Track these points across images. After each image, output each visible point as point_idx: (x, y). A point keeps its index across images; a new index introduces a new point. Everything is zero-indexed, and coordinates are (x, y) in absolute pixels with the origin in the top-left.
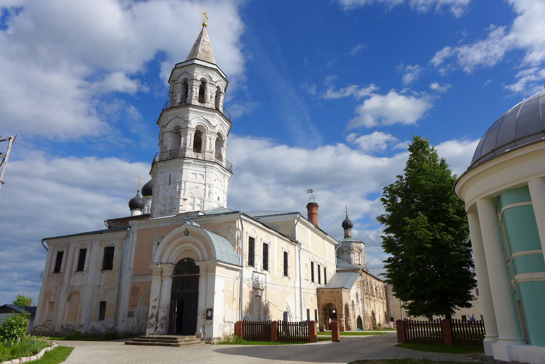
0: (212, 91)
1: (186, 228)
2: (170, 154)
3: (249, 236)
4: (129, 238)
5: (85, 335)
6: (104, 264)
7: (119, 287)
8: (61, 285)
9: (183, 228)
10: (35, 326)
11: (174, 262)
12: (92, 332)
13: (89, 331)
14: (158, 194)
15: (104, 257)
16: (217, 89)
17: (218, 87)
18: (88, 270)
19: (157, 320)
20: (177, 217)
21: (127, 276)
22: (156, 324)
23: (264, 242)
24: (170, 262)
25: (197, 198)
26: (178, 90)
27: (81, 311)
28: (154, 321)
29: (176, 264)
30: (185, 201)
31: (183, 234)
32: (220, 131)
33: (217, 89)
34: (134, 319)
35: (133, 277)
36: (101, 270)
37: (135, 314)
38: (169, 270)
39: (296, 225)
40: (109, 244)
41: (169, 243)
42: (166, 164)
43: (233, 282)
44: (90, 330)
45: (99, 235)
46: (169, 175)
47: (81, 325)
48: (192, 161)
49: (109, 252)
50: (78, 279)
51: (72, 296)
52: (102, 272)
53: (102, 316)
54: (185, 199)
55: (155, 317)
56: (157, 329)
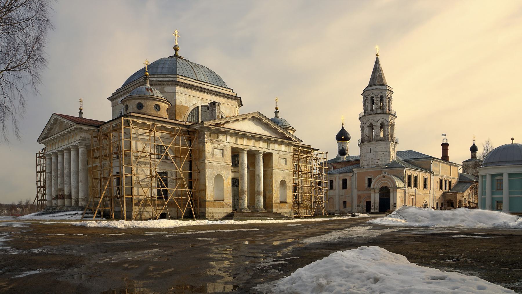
1: (384, 175)
7: (352, 196)
9: (382, 175)
14: (365, 157)
24: (377, 187)
26: (369, 103)
27: (335, 205)
34: (361, 207)
37: (360, 205)
38: (377, 191)
39: (431, 164)
40: (344, 178)
48: (380, 142)
49: (345, 182)
53: (345, 207)
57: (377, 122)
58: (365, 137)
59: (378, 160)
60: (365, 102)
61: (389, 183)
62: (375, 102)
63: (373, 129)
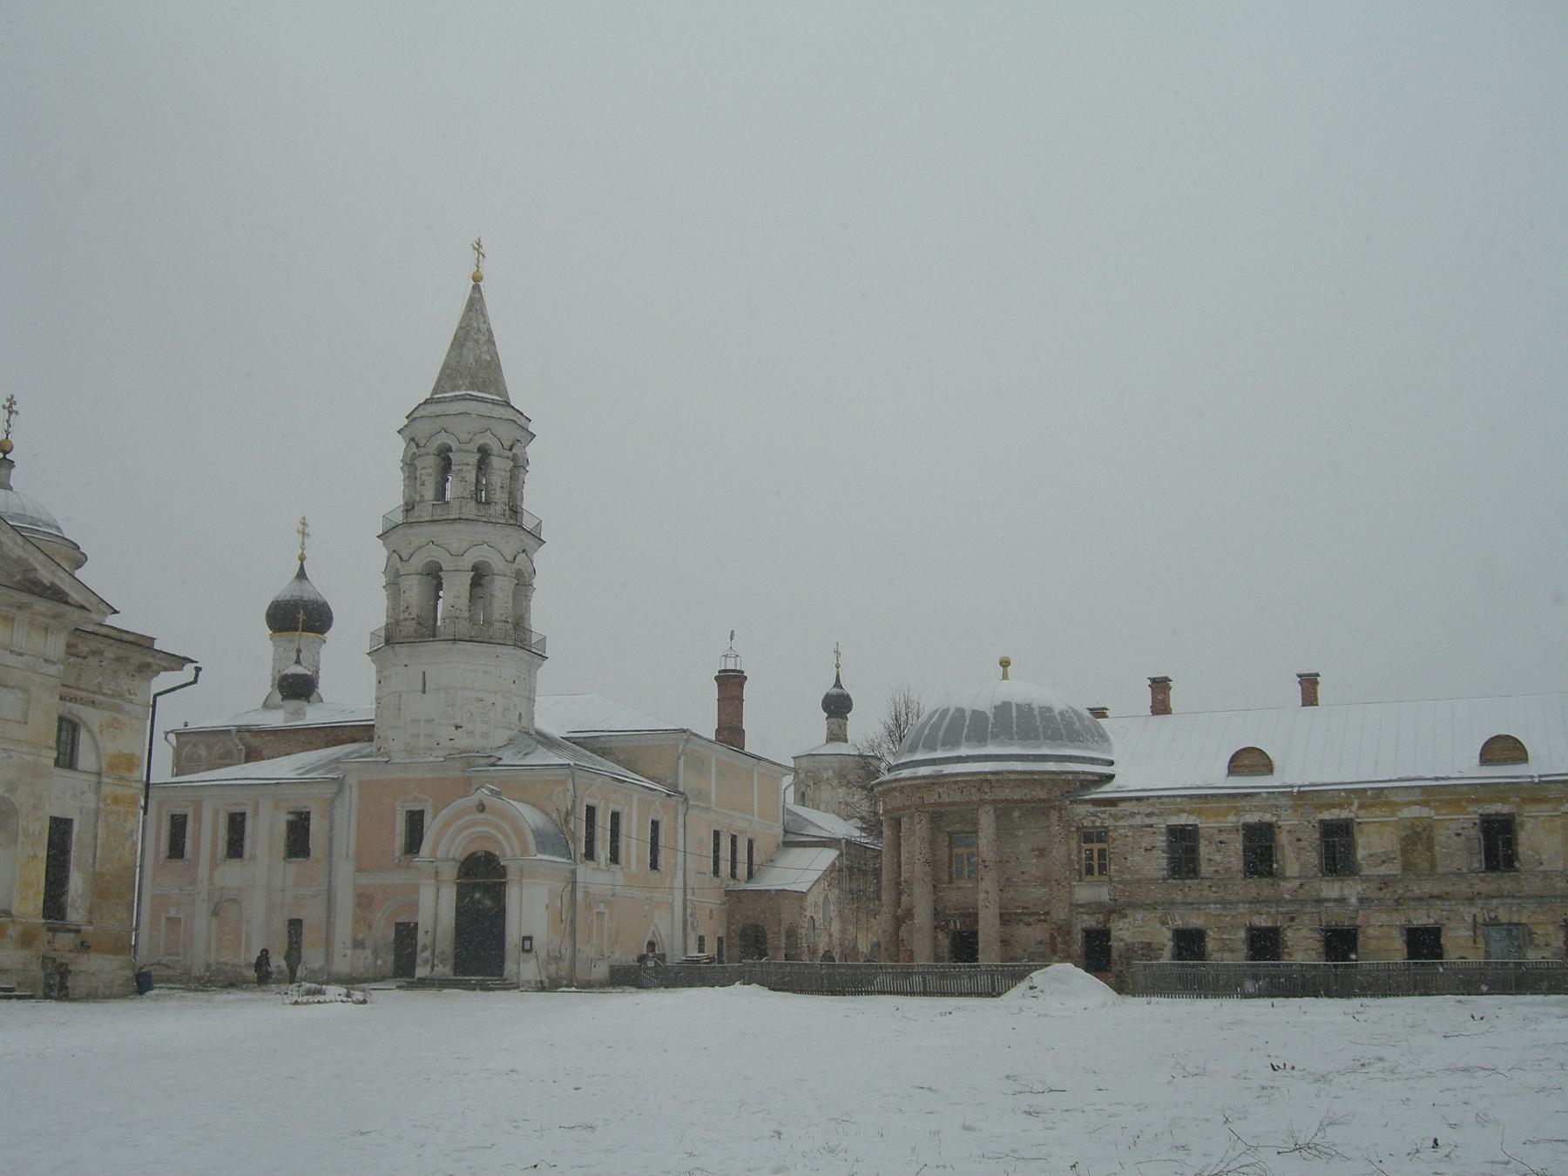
9: (474, 799)
10: (142, 965)
11: (457, 858)
14: (399, 709)
18: (253, 858)
21: (345, 872)
24: (451, 856)
29: (462, 859)
30: (459, 729)
31: (475, 809)
38: (450, 872)
41: (447, 825)
50: (232, 874)
56: (436, 968)
58: (402, 618)
59: (457, 727)
60: (410, 464)
61: (500, 836)
63: (439, 586)
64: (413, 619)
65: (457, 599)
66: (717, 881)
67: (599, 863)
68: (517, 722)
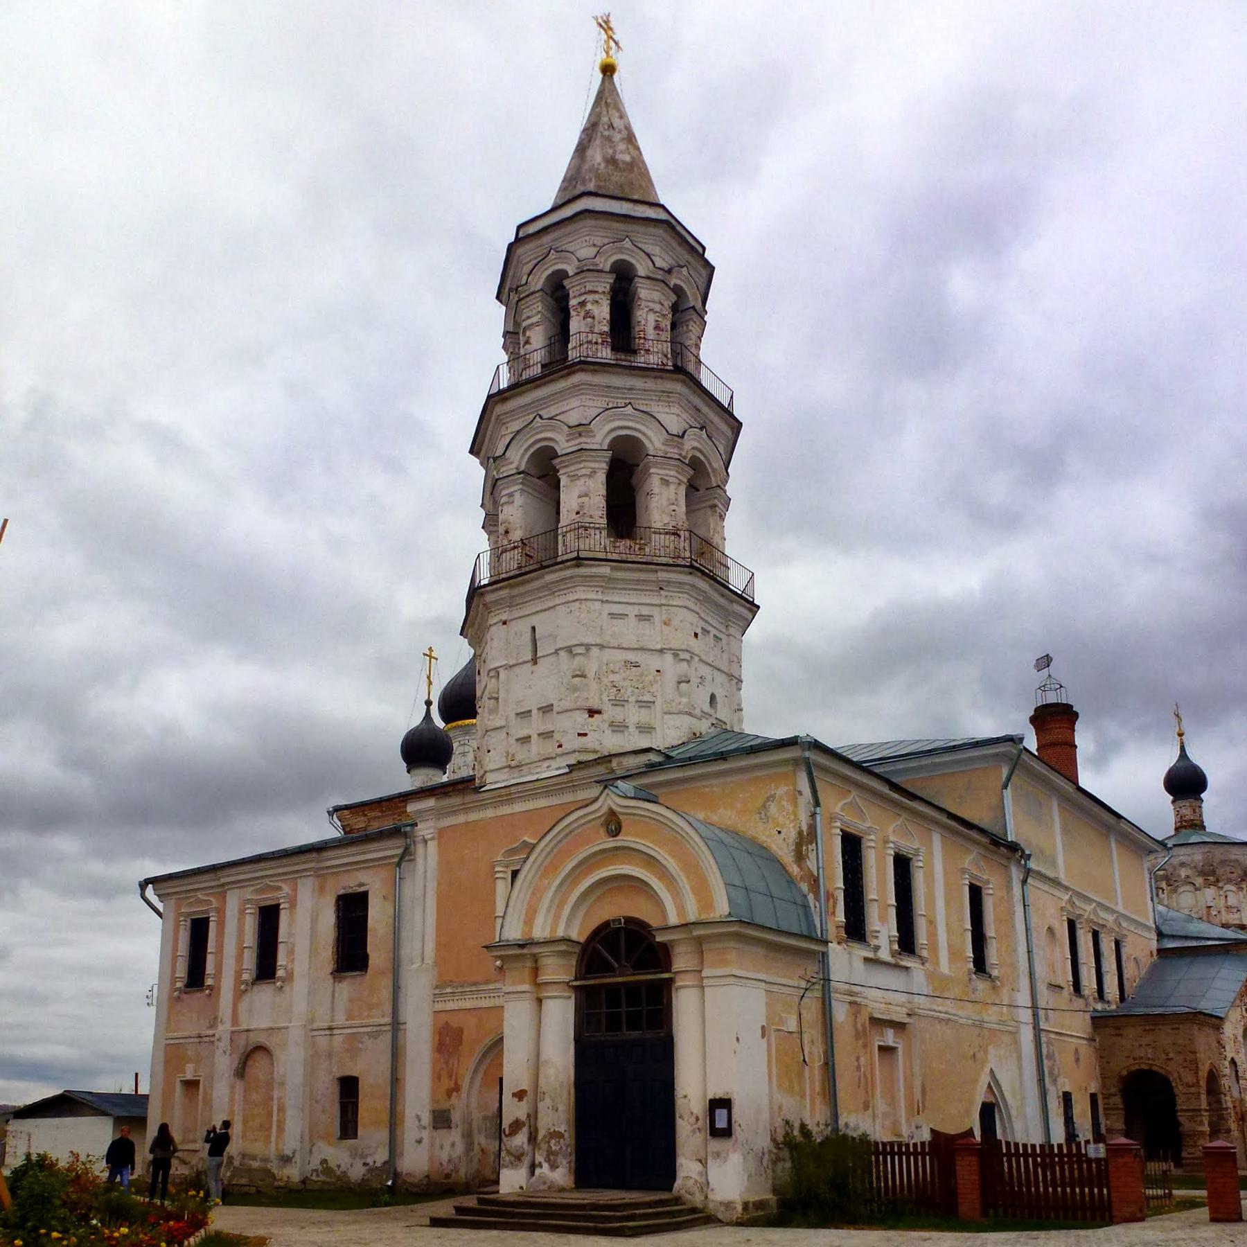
0: (657, 307)
2: (526, 555)
3: (842, 830)
4: (414, 860)
5: (301, 1186)
6: (338, 951)
7: (396, 1026)
8: (213, 1025)
12: (322, 1178)
13: (312, 1175)
14: (497, 699)
15: (339, 927)
16: (674, 298)
17: (678, 290)
18: (290, 977)
19: (532, 1138)
20: (569, 776)
22: (530, 1155)
23: (897, 851)
25: (637, 701)
27: (281, 1109)
28: (523, 1143)
29: (582, 940)
30: (596, 716)
32: (701, 451)
33: (674, 298)
35: (437, 991)
36: (331, 973)
37: (456, 1117)
38: (558, 970)
40: (349, 883)
42: (515, 591)
43: (797, 1000)
44: (316, 1170)
45: (314, 855)
46: (530, 629)
47: (288, 1156)
48: (605, 570)
51: (250, 1063)
52: (334, 978)
53: (349, 1128)
54: (596, 707)
55: (525, 1130)
56: (538, 1171)
57: (580, 429)
59: (592, 712)
62: (573, 302)
64: (515, 548)
65: (586, 499)
66: (1079, 1003)
67: (877, 948)
68: (707, 708)
